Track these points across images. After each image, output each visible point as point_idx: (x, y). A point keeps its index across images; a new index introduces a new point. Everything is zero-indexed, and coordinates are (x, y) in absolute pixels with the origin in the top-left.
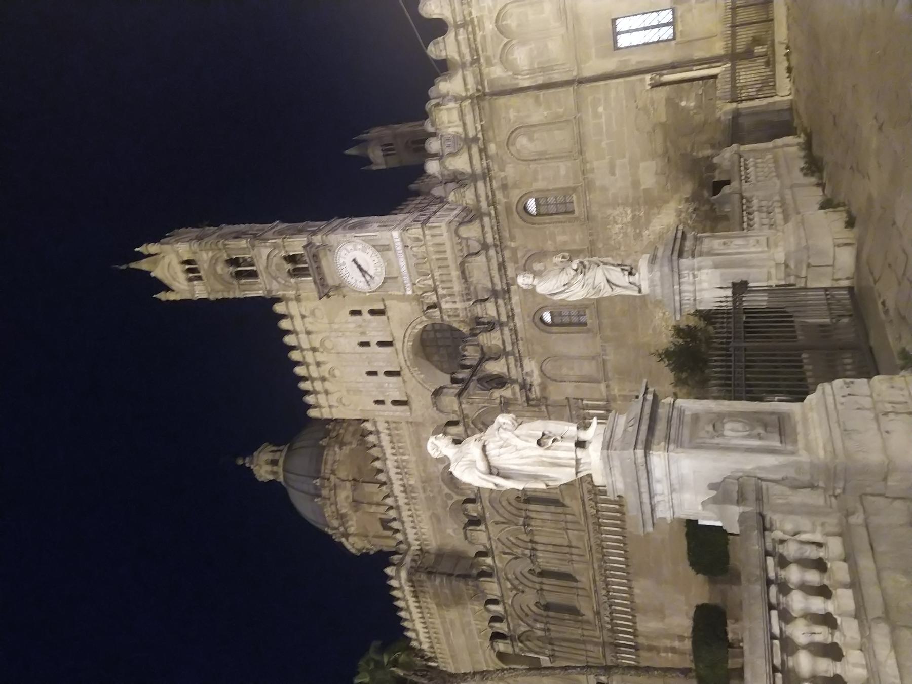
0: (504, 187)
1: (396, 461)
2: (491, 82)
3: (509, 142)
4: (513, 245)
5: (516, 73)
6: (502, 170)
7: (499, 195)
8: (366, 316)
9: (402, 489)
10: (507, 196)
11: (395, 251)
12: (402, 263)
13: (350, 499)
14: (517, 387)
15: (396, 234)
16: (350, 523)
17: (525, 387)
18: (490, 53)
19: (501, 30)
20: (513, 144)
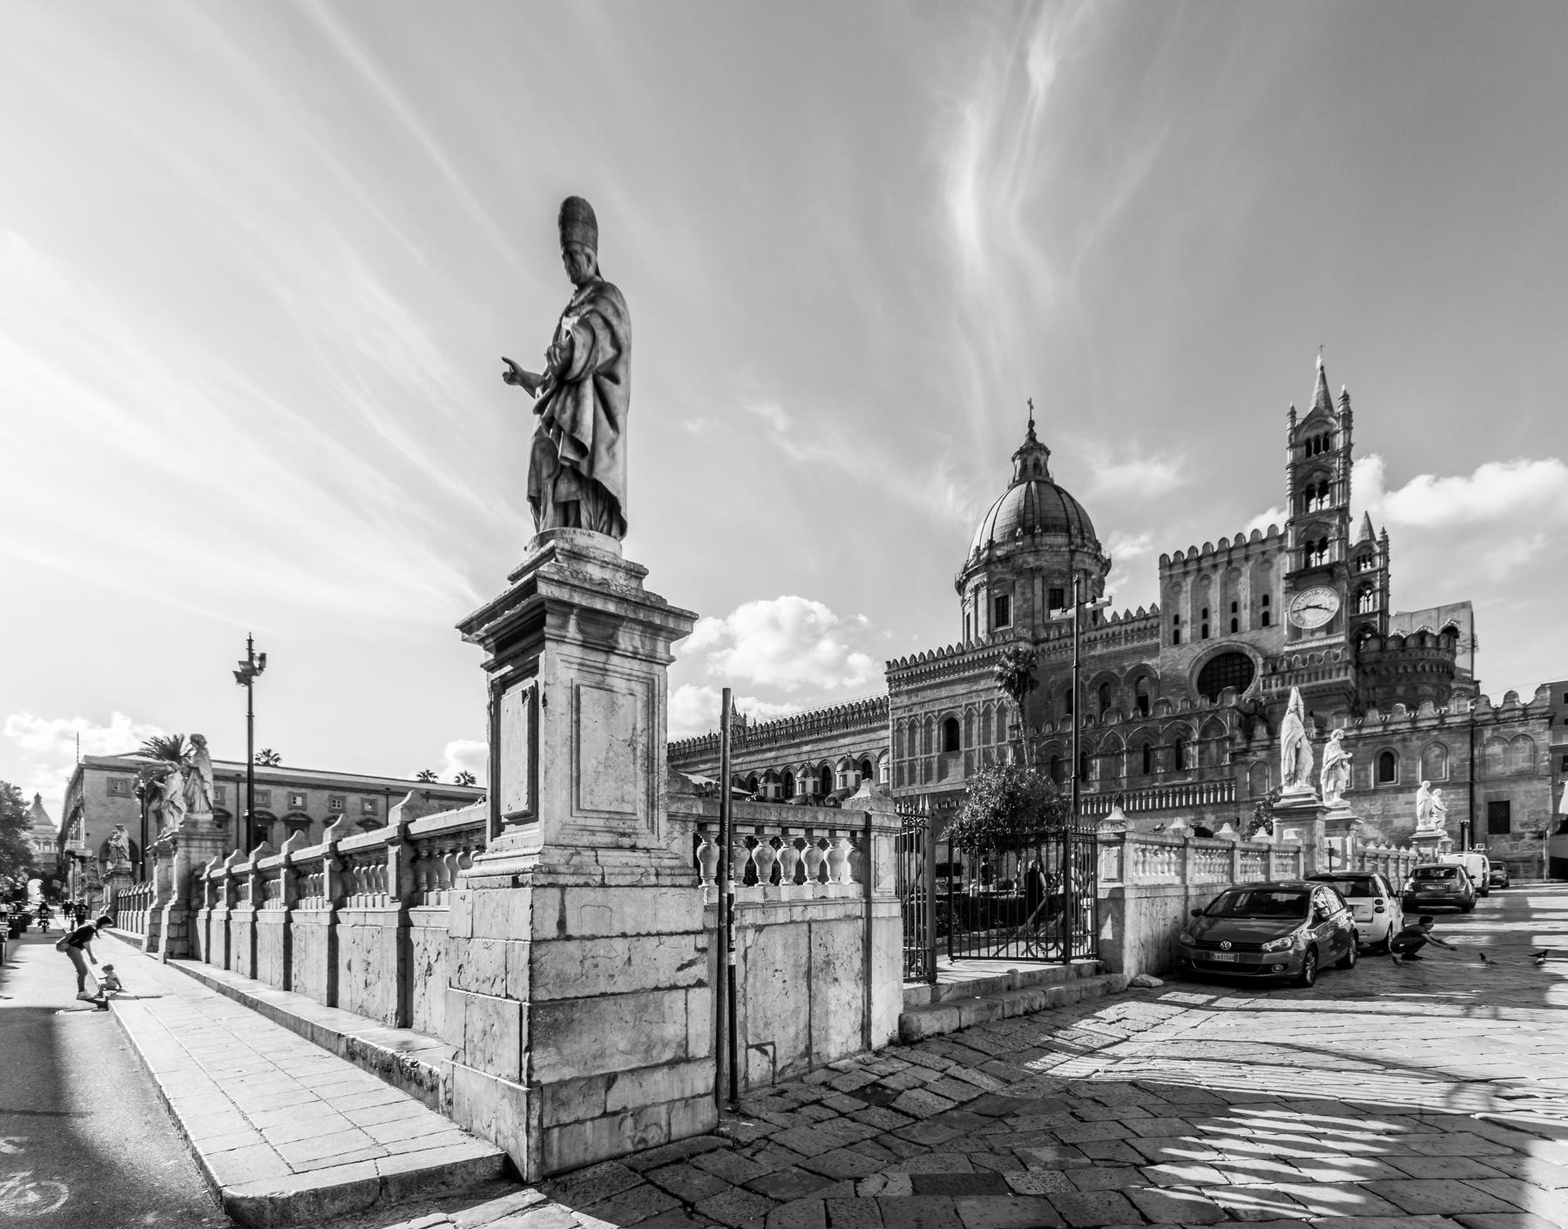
0: (1404, 740)
1: (1120, 633)
2: (1482, 731)
3: (1437, 743)
4: (1360, 745)
5: (1485, 746)
6: (1417, 739)
7: (1398, 737)
8: (1262, 611)
9: (1092, 638)
10: (1397, 741)
11: (1326, 638)
12: (1314, 644)
13: (1025, 566)
14: (1244, 746)
15: (1342, 639)
16: (1000, 566)
17: (1246, 752)
18: (1502, 730)
19: (1516, 738)
20: (1436, 746)
